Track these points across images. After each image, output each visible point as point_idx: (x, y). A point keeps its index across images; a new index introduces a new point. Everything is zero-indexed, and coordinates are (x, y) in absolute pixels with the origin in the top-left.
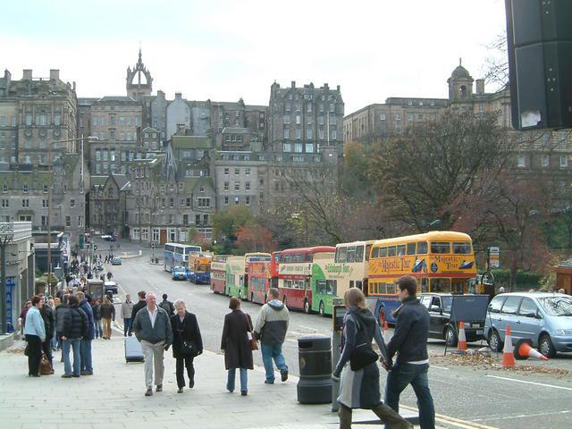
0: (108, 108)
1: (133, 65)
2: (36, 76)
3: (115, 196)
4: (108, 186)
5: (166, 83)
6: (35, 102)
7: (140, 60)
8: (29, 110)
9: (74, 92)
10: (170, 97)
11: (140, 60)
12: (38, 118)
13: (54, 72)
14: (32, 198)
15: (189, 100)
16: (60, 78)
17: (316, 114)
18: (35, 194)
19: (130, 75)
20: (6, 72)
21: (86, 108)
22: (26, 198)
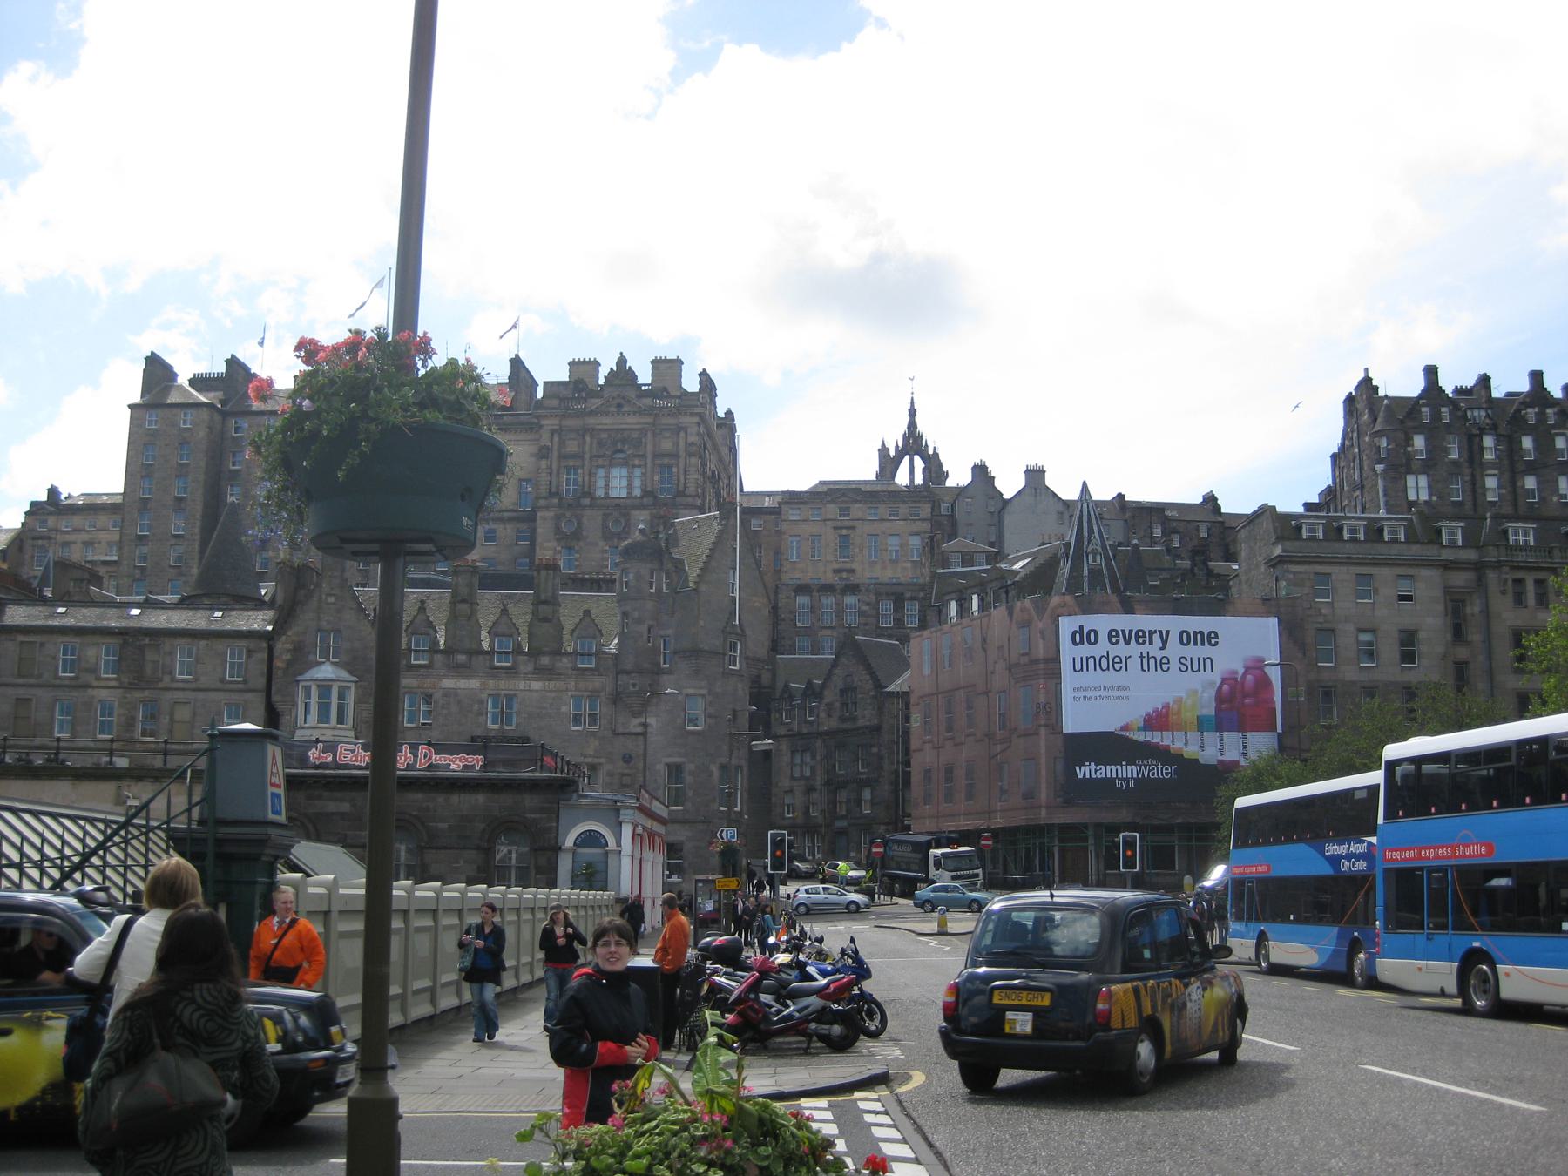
0: (832, 510)
1: (894, 437)
3: (866, 716)
4: (838, 681)
6: (591, 421)
7: (912, 425)
8: (572, 447)
10: (1009, 484)
11: (912, 425)
12: (601, 472)
17: (1512, 465)
18: (542, 672)
20: (517, 363)
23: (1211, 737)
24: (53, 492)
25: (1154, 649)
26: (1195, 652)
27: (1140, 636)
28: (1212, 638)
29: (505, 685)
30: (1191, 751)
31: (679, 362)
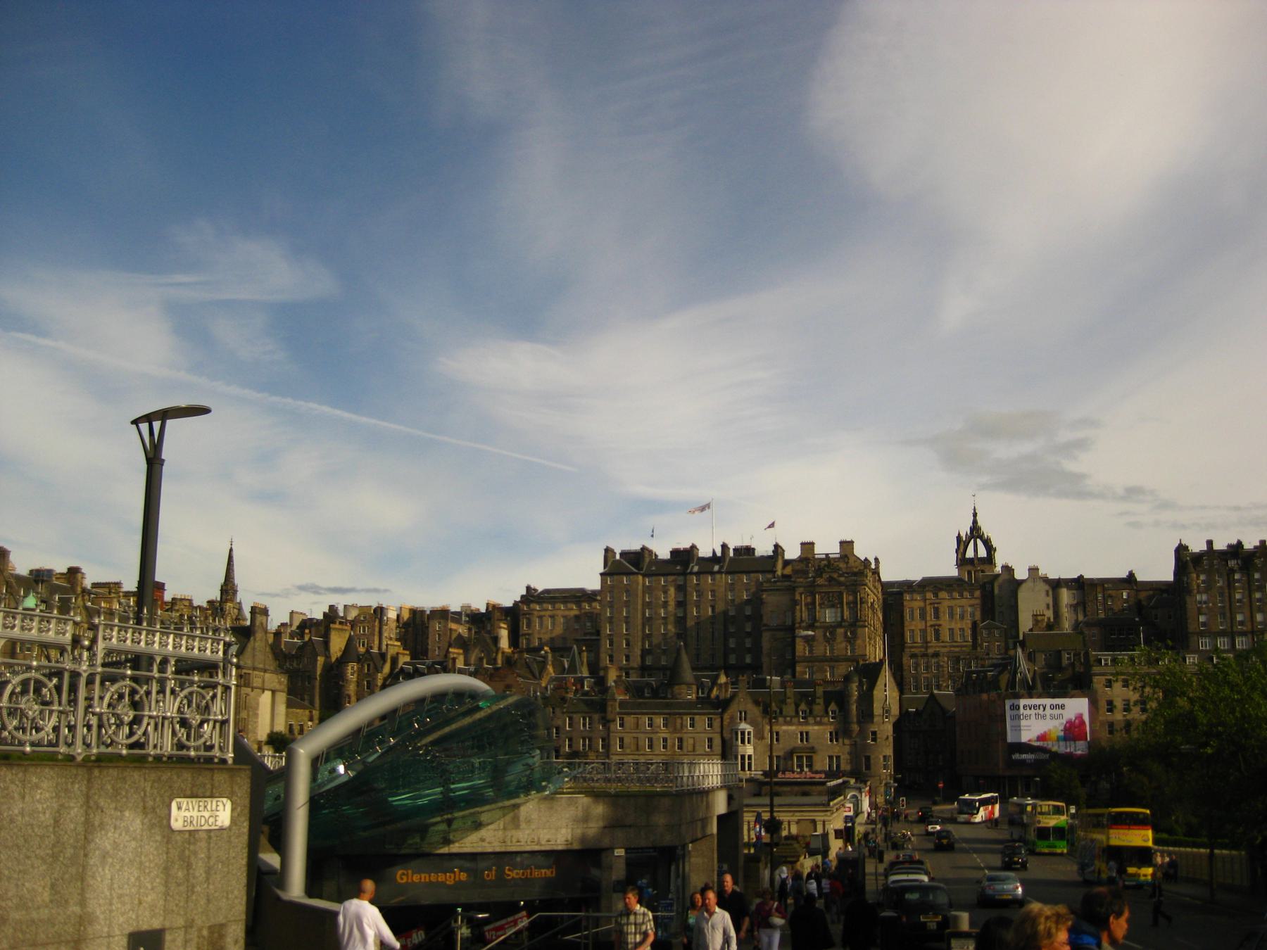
1: (965, 530)
2: (820, 550)
5: (1015, 554)
7: (975, 522)
9: (876, 572)
10: (1021, 574)
11: (975, 522)
13: (847, 545)
14: (813, 729)
15: (1051, 576)
16: (856, 553)
18: (819, 723)
19: (962, 544)
20: (777, 546)
21: (896, 596)
22: (805, 728)
23: (1062, 743)
24: (528, 588)
25: (1041, 711)
26: (1056, 712)
27: (1035, 707)
28: (1063, 707)
29: (805, 728)
30: (1055, 749)
31: (852, 542)
